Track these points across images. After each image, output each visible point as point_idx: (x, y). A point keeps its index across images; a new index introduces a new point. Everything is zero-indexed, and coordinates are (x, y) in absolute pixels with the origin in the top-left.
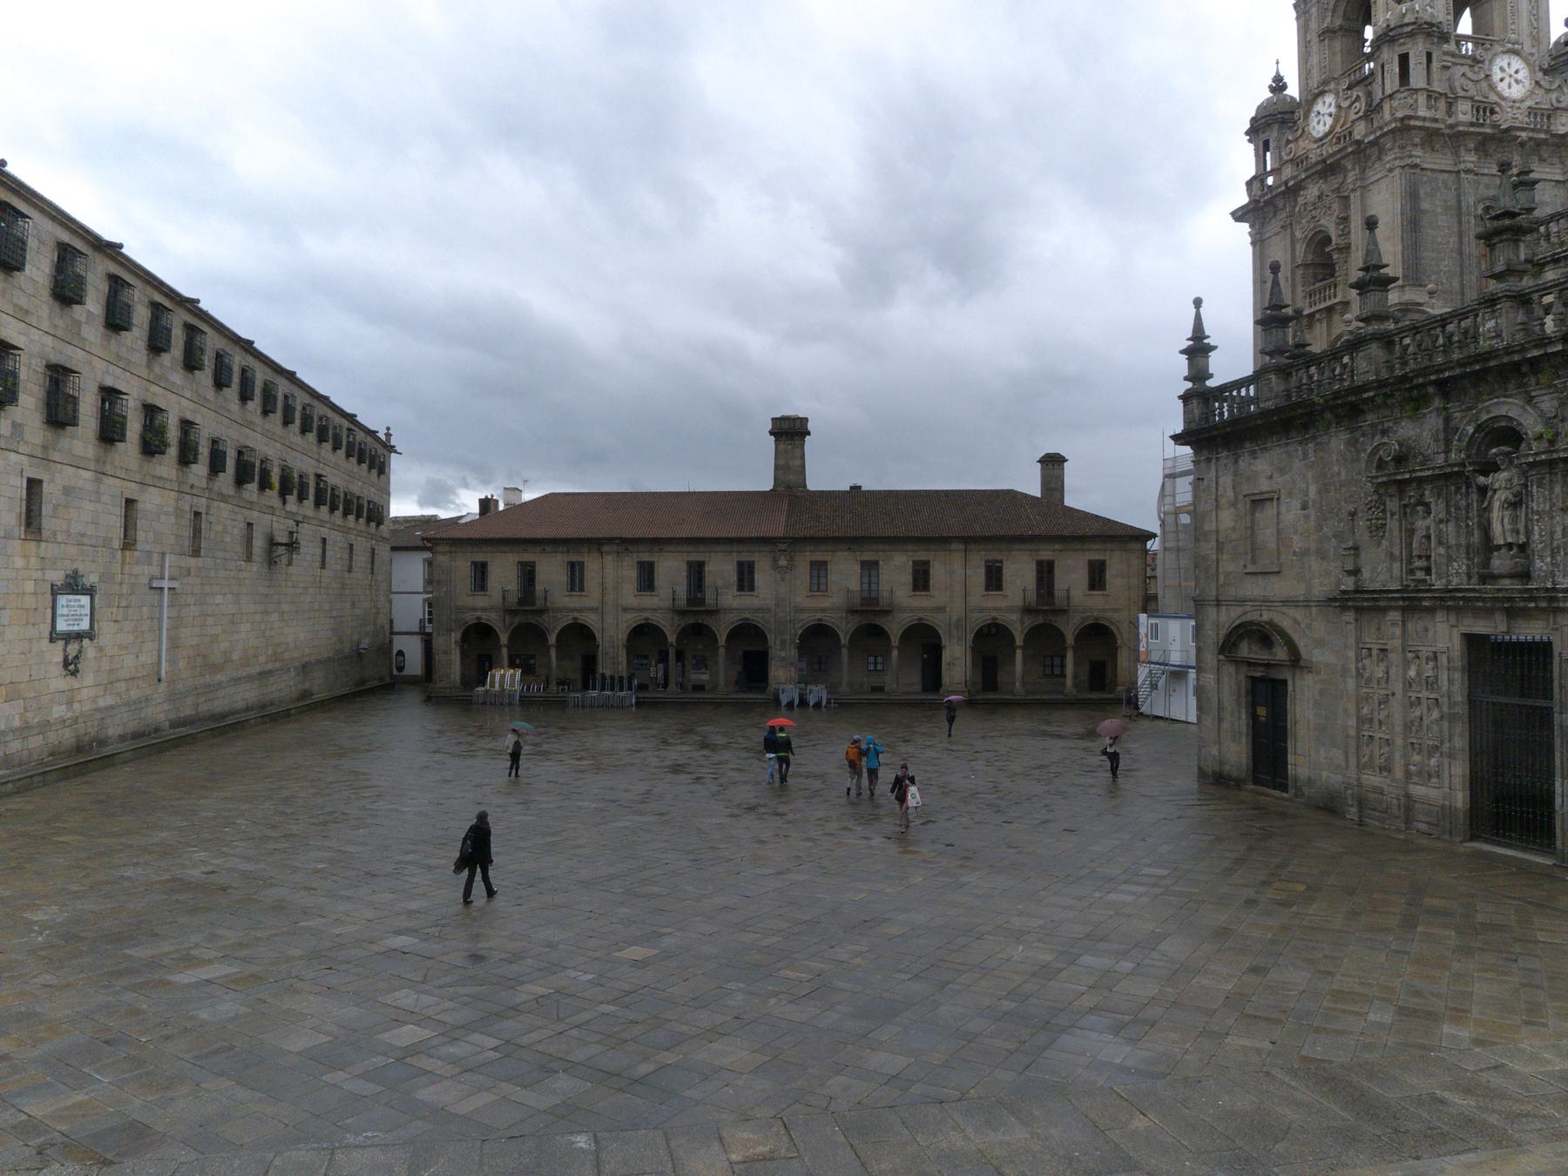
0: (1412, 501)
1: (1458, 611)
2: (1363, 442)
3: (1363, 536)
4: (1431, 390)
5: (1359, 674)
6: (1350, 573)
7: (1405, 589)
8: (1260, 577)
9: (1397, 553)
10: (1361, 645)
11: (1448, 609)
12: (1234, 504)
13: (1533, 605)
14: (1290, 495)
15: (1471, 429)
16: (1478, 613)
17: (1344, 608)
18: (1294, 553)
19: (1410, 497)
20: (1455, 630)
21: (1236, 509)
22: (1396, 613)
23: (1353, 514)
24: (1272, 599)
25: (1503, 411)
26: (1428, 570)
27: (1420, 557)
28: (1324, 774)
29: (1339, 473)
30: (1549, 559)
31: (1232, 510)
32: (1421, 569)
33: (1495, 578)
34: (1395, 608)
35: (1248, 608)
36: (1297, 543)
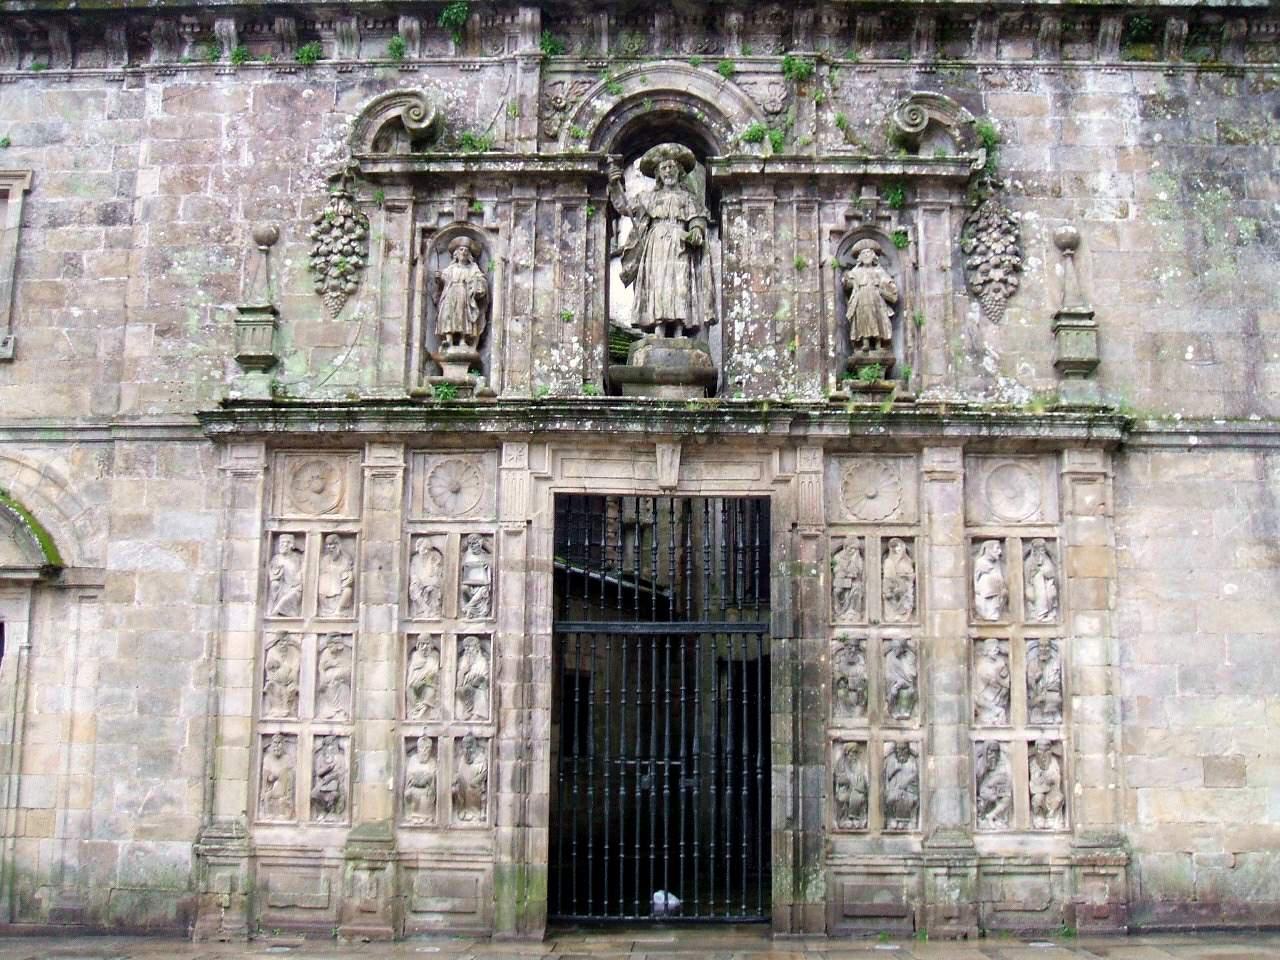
0: (444, 223)
1: (562, 442)
2: (310, 101)
5: (264, 587)
6: (247, 363)
7: (417, 399)
9: (397, 328)
10: (275, 527)
11: (536, 439)
13: (759, 429)
15: (604, 105)
16: (602, 445)
19: (442, 215)
20: (544, 486)
22: (391, 453)
25: (681, 83)
26: (476, 366)
27: (457, 337)
29: (235, 153)
30: (771, 353)
32: (456, 360)
33: (645, 379)
34: (384, 440)
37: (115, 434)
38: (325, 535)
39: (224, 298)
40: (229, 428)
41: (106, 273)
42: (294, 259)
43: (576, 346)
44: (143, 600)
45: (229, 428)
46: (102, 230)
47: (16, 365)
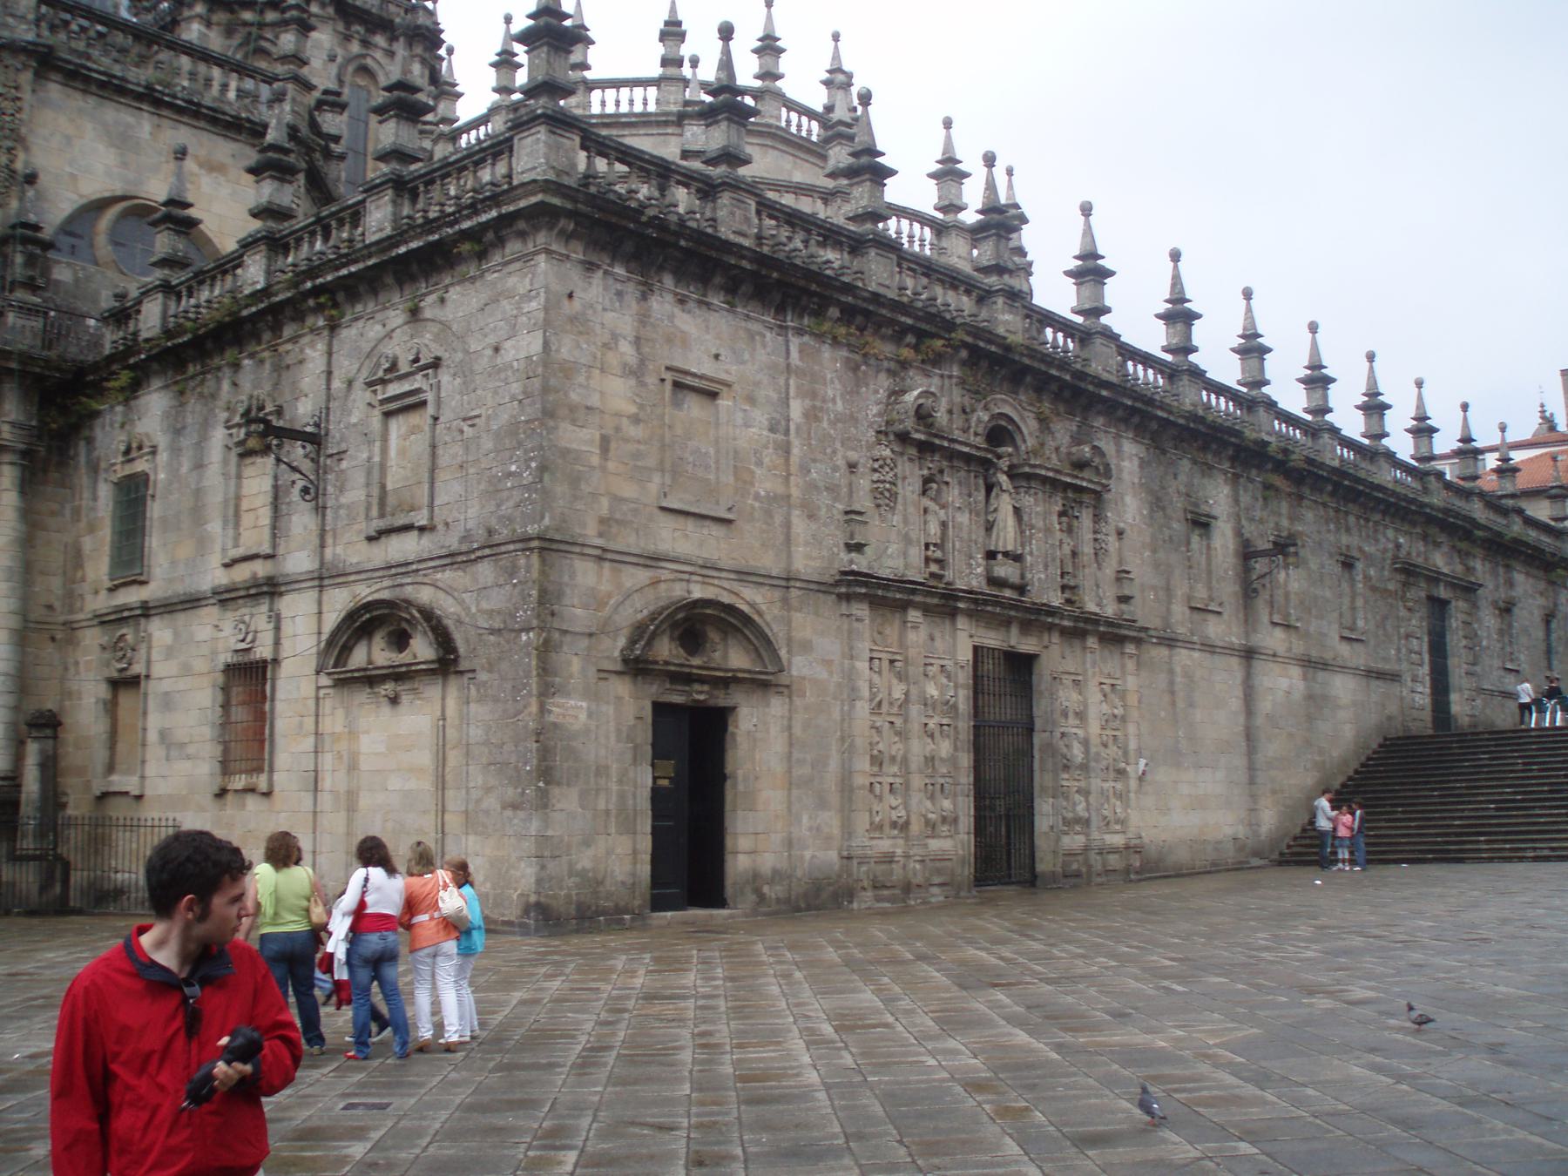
2: (865, 373)
3: (864, 502)
4: (964, 354)
8: (690, 524)
12: (636, 372)
14: (751, 400)
17: (848, 598)
18: (757, 497)
19: (929, 468)
21: (642, 384)
23: (852, 466)
24: (721, 565)
28: (808, 854)
29: (834, 400)
31: (632, 382)
35: (665, 575)
36: (765, 484)
37: (792, 583)
38: (892, 662)
39: (836, 499)
40: (863, 590)
41: (775, 468)
42: (864, 483)
43: (980, 561)
44: (810, 697)
45: (863, 590)
46: (772, 435)
47: (733, 526)
